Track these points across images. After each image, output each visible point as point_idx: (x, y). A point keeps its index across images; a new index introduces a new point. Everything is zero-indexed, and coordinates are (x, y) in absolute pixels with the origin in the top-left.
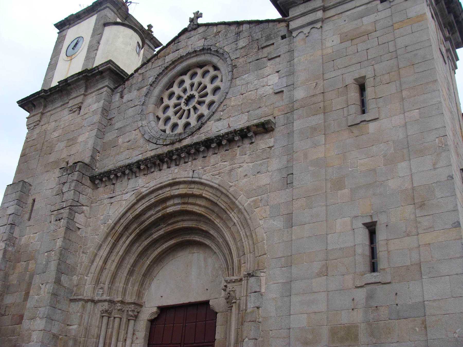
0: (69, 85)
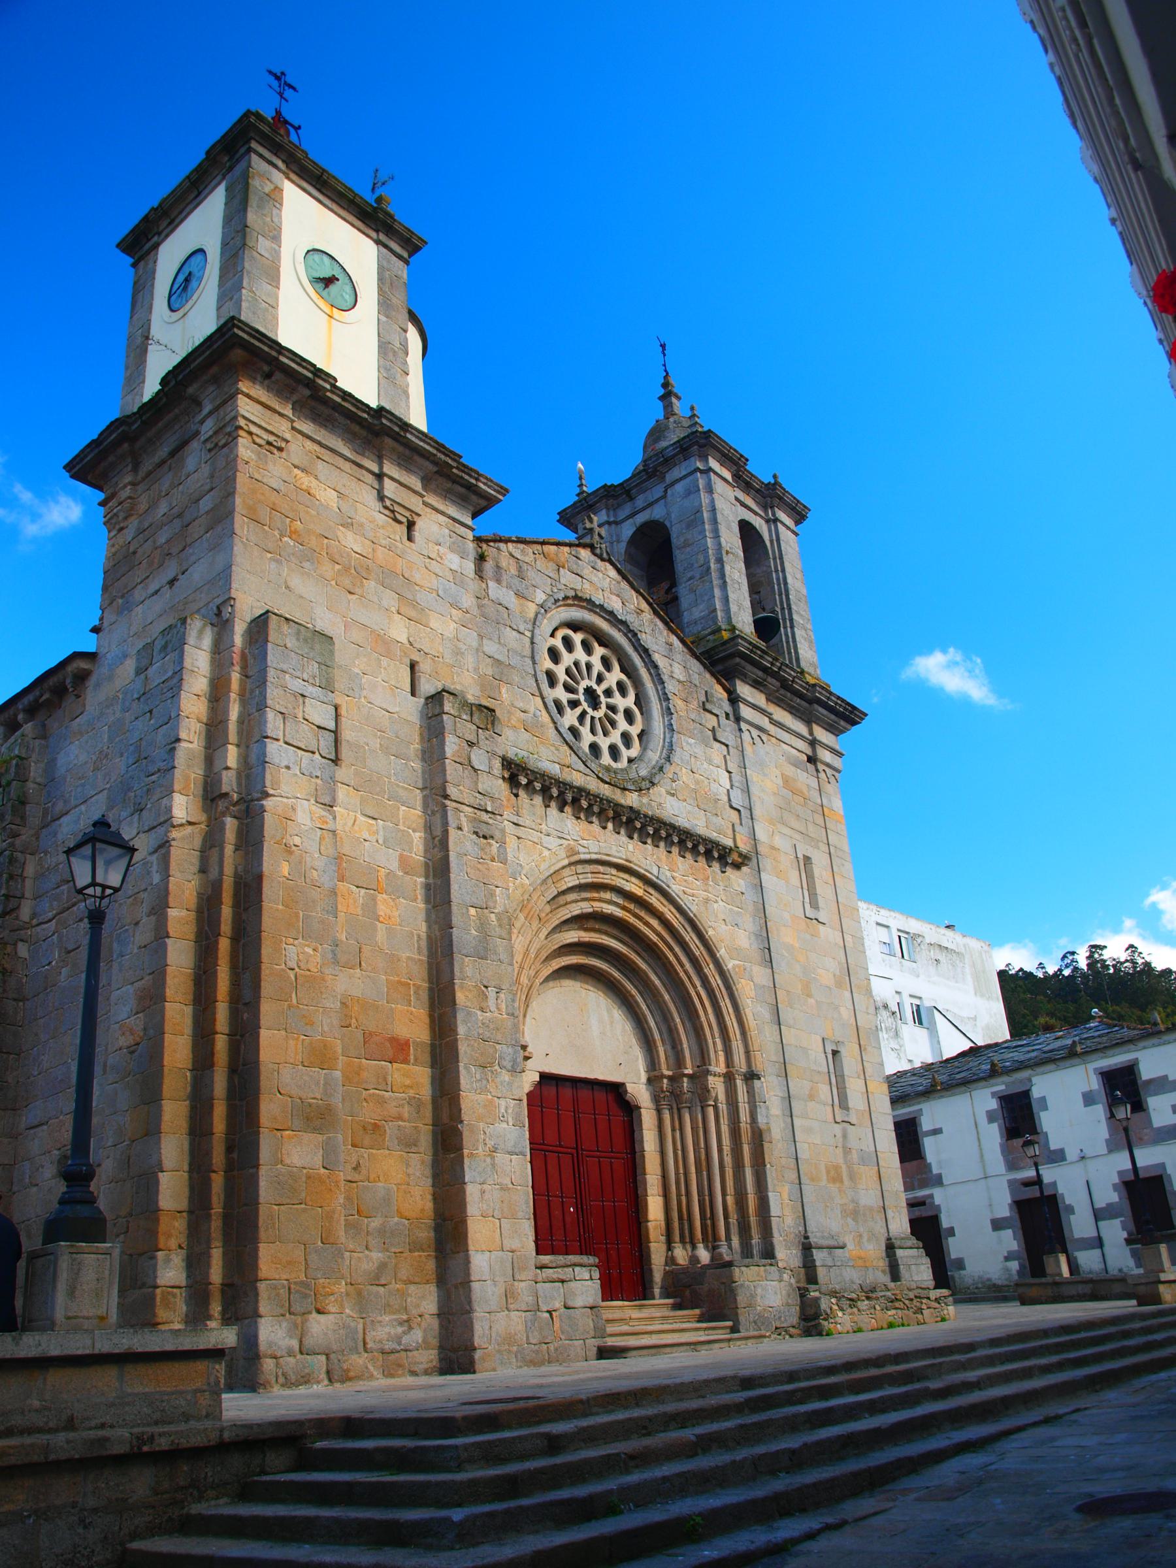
0: (396, 437)
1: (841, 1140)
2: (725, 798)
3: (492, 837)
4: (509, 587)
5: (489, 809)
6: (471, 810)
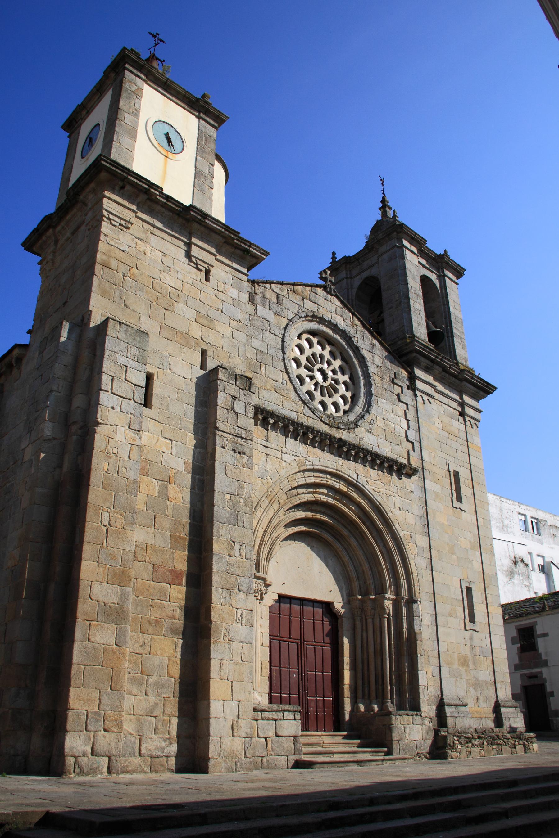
0: (200, 223)
1: (469, 640)
2: (404, 435)
3: (244, 453)
4: (270, 309)
5: (243, 436)
6: (231, 436)
